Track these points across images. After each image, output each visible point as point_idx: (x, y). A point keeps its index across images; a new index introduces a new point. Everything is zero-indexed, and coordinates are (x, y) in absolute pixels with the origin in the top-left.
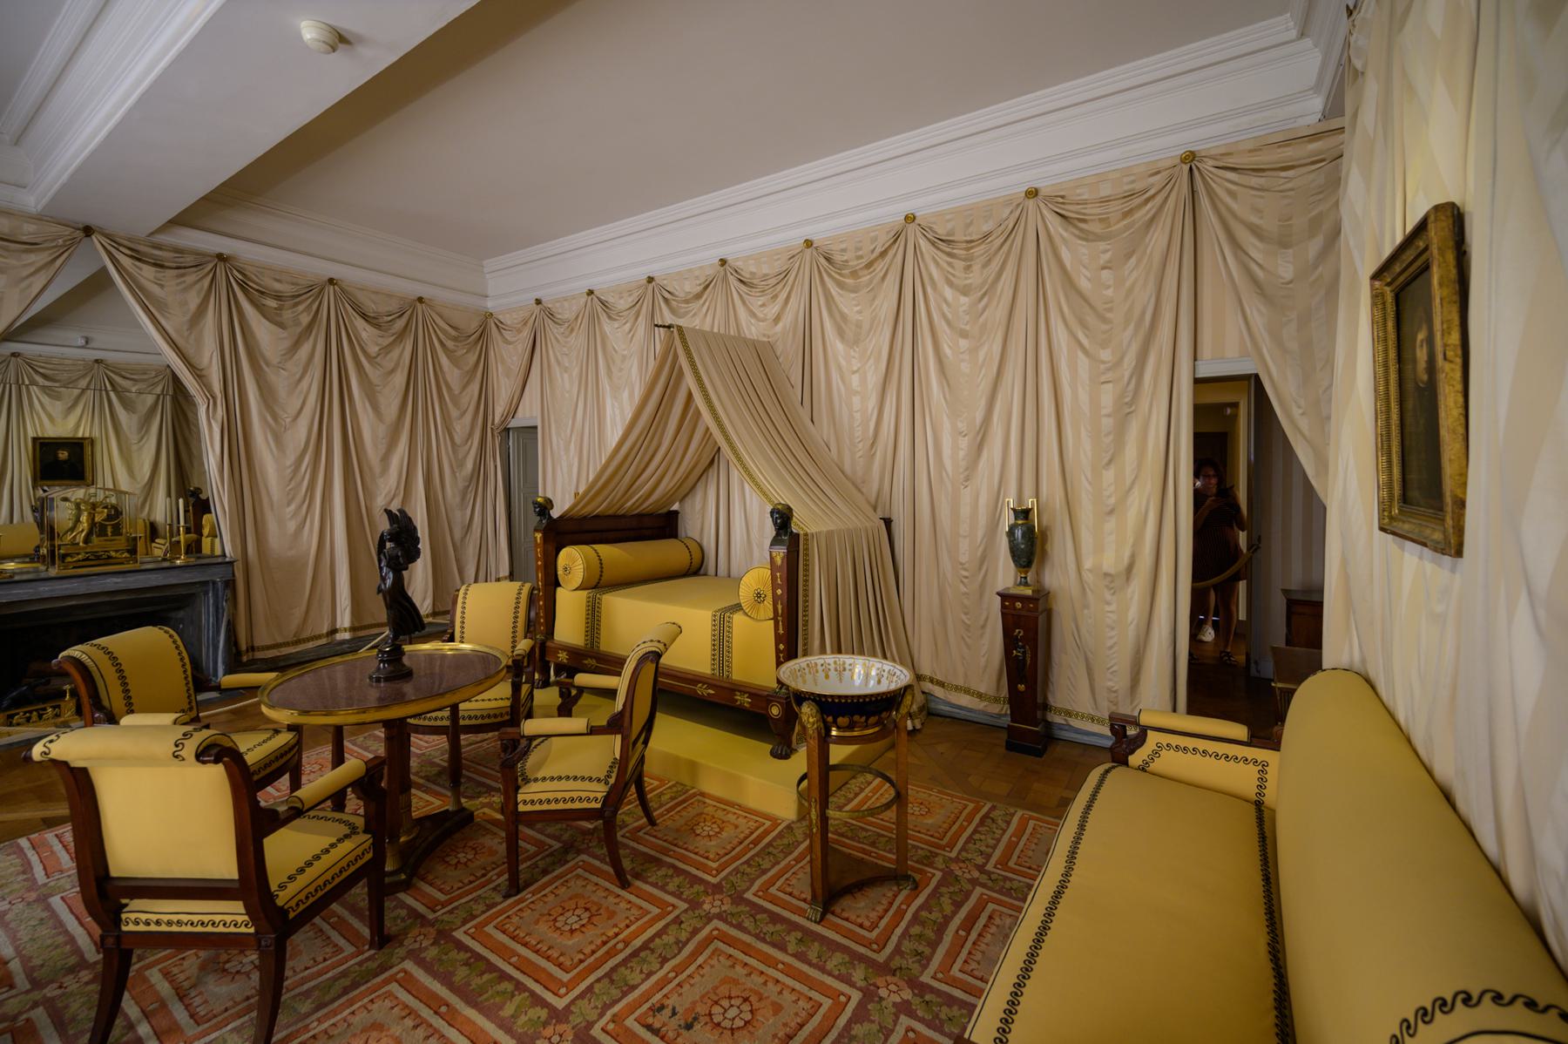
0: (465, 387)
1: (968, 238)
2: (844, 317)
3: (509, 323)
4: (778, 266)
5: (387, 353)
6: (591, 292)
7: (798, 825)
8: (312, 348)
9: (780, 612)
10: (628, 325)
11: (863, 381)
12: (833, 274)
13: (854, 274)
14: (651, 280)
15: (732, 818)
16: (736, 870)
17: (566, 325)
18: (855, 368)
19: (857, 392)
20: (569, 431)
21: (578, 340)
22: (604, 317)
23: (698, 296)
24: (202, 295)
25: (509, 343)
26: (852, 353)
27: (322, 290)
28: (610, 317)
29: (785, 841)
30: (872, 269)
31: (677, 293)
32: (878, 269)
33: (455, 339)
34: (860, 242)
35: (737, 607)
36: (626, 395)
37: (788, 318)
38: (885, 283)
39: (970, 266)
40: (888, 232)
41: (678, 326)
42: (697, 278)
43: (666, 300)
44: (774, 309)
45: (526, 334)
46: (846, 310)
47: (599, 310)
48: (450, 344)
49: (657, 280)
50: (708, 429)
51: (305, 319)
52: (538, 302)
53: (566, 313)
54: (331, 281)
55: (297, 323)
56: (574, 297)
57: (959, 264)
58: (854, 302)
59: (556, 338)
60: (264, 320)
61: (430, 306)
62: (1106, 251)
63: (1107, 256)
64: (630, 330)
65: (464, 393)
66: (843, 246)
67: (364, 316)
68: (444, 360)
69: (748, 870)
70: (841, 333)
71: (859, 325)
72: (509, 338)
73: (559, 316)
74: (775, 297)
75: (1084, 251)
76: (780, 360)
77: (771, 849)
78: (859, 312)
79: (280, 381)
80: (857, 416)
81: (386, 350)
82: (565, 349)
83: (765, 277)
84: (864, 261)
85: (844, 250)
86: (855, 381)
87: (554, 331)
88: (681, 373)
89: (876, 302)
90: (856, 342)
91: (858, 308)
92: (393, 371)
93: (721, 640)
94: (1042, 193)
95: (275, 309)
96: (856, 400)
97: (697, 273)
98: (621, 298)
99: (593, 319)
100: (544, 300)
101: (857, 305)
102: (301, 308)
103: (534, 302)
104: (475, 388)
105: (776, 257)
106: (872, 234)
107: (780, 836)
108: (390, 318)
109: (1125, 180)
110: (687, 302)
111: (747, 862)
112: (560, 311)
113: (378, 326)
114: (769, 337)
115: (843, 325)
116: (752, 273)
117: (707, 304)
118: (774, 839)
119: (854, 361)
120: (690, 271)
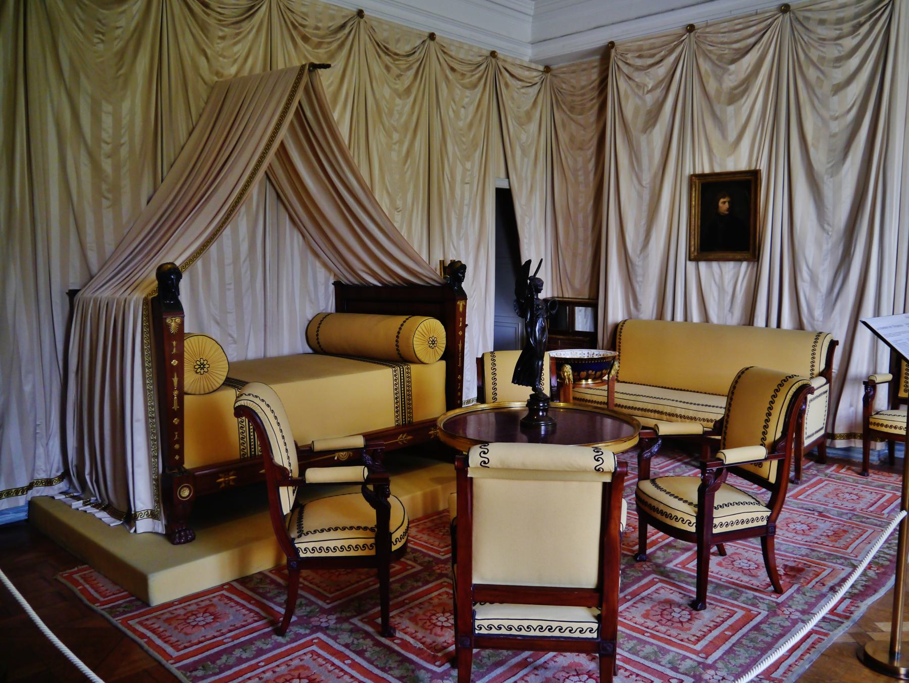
1: (398, 52)
34: (320, 13)
39: (401, 75)
57: (395, 71)
62: (467, 97)
63: (466, 100)
66: (304, 10)
75: (458, 92)
94: (437, 38)
109: (471, 53)
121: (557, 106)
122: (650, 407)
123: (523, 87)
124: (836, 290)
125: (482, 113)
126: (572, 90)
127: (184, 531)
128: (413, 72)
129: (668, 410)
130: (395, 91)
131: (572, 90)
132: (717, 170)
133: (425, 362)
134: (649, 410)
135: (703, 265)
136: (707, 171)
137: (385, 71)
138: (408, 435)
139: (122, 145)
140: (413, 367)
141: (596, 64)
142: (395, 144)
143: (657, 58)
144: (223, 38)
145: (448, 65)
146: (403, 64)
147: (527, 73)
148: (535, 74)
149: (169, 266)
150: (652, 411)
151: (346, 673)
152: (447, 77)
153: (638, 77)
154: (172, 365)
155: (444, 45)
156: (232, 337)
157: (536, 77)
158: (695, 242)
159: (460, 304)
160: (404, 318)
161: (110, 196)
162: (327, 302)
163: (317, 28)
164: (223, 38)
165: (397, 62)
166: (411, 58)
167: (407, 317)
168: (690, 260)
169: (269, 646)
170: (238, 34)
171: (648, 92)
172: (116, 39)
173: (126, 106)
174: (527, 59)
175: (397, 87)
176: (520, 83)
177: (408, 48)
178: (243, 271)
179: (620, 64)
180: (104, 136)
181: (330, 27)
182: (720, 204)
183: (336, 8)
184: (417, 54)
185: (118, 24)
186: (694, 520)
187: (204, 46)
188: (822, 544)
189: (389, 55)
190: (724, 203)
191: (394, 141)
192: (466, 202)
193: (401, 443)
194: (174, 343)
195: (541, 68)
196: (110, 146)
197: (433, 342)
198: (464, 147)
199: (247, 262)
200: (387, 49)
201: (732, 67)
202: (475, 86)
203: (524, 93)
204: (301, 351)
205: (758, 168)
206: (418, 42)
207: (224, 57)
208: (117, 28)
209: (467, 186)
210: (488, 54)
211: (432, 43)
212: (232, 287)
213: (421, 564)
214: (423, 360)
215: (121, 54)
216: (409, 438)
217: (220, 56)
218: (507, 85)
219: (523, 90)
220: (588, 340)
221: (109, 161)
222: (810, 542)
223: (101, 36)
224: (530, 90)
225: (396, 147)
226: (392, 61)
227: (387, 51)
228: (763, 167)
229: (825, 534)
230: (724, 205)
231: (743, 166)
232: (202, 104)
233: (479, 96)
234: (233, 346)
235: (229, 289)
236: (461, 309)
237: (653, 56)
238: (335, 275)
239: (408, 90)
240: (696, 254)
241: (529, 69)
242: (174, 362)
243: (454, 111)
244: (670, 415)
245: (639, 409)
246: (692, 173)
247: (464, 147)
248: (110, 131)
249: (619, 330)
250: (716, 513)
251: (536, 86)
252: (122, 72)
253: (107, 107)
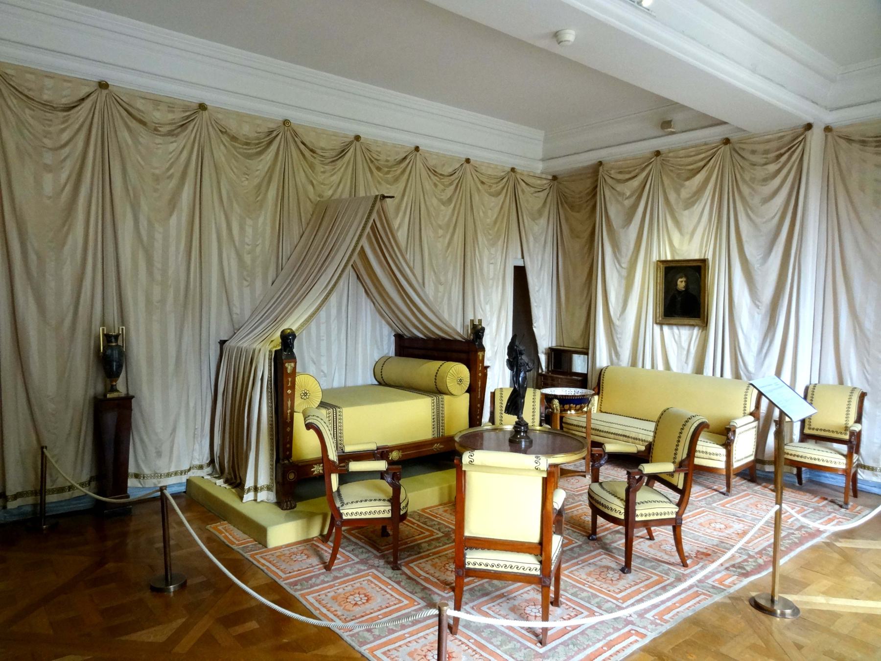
1: (443, 173)
34: (389, 151)
42: (258, 125)
57: (441, 187)
62: (493, 202)
63: (492, 204)
66: (379, 149)
94: (472, 162)
97: (259, 122)
121: (562, 207)
122: (620, 432)
123: (536, 192)
124: (764, 351)
125: (504, 213)
126: (573, 194)
127: (290, 501)
128: (453, 187)
129: (633, 435)
130: (441, 201)
131: (573, 194)
132: (677, 258)
133: (454, 394)
134: (619, 435)
135: (666, 328)
136: (669, 258)
137: (433, 187)
138: (441, 444)
139: (258, 245)
140: (446, 397)
141: (589, 175)
142: (440, 237)
143: (632, 174)
144: (324, 172)
145: (479, 180)
146: (446, 181)
147: (539, 182)
148: (545, 182)
149: (289, 331)
150: (621, 435)
151: (388, 593)
152: (478, 189)
153: (619, 187)
154: (288, 393)
155: (477, 166)
156: (323, 372)
157: (545, 184)
158: (660, 310)
159: (480, 354)
160: (440, 363)
161: (249, 279)
162: (389, 347)
163: (387, 161)
164: (324, 172)
165: (442, 180)
166: (451, 177)
167: (443, 362)
168: (657, 323)
169: (342, 575)
170: (334, 169)
171: (627, 198)
172: (256, 177)
173: (261, 220)
174: (539, 172)
175: (442, 197)
176: (533, 189)
177: (450, 170)
178: (333, 327)
179: (606, 177)
180: (247, 240)
181: (395, 160)
182: (679, 283)
183: (400, 146)
184: (456, 174)
185: (258, 168)
186: (623, 511)
187: (311, 178)
188: (731, 539)
189: (436, 176)
190: (682, 282)
191: (440, 235)
192: (491, 277)
194: (290, 379)
195: (550, 177)
196: (250, 247)
197: (461, 381)
198: (490, 237)
199: (336, 321)
200: (435, 172)
201: (687, 183)
202: (498, 194)
203: (536, 197)
204: (370, 383)
205: (706, 258)
206: (458, 166)
207: (325, 185)
208: (258, 170)
209: (492, 267)
210: (509, 170)
211: (467, 165)
212: (325, 338)
213: (442, 532)
214: (453, 393)
215: (259, 186)
216: (442, 446)
217: (322, 184)
218: (523, 191)
219: (536, 195)
220: (582, 381)
221: (249, 255)
222: (723, 536)
223: (247, 176)
224: (541, 194)
225: (441, 239)
226: (439, 180)
227: (435, 173)
228: (710, 257)
229: (736, 532)
230: (681, 284)
231: (697, 257)
232: (309, 216)
233: (502, 200)
234: (324, 378)
235: (323, 340)
236: (481, 358)
237: (630, 172)
238: (395, 331)
239: (450, 200)
240: (660, 319)
241: (540, 178)
242: (289, 391)
243: (483, 212)
244: (634, 439)
245: (612, 433)
246: (658, 259)
247: (490, 237)
248: (250, 237)
249: (602, 373)
250: (637, 507)
251: (545, 191)
252: (259, 199)
253: (249, 222)
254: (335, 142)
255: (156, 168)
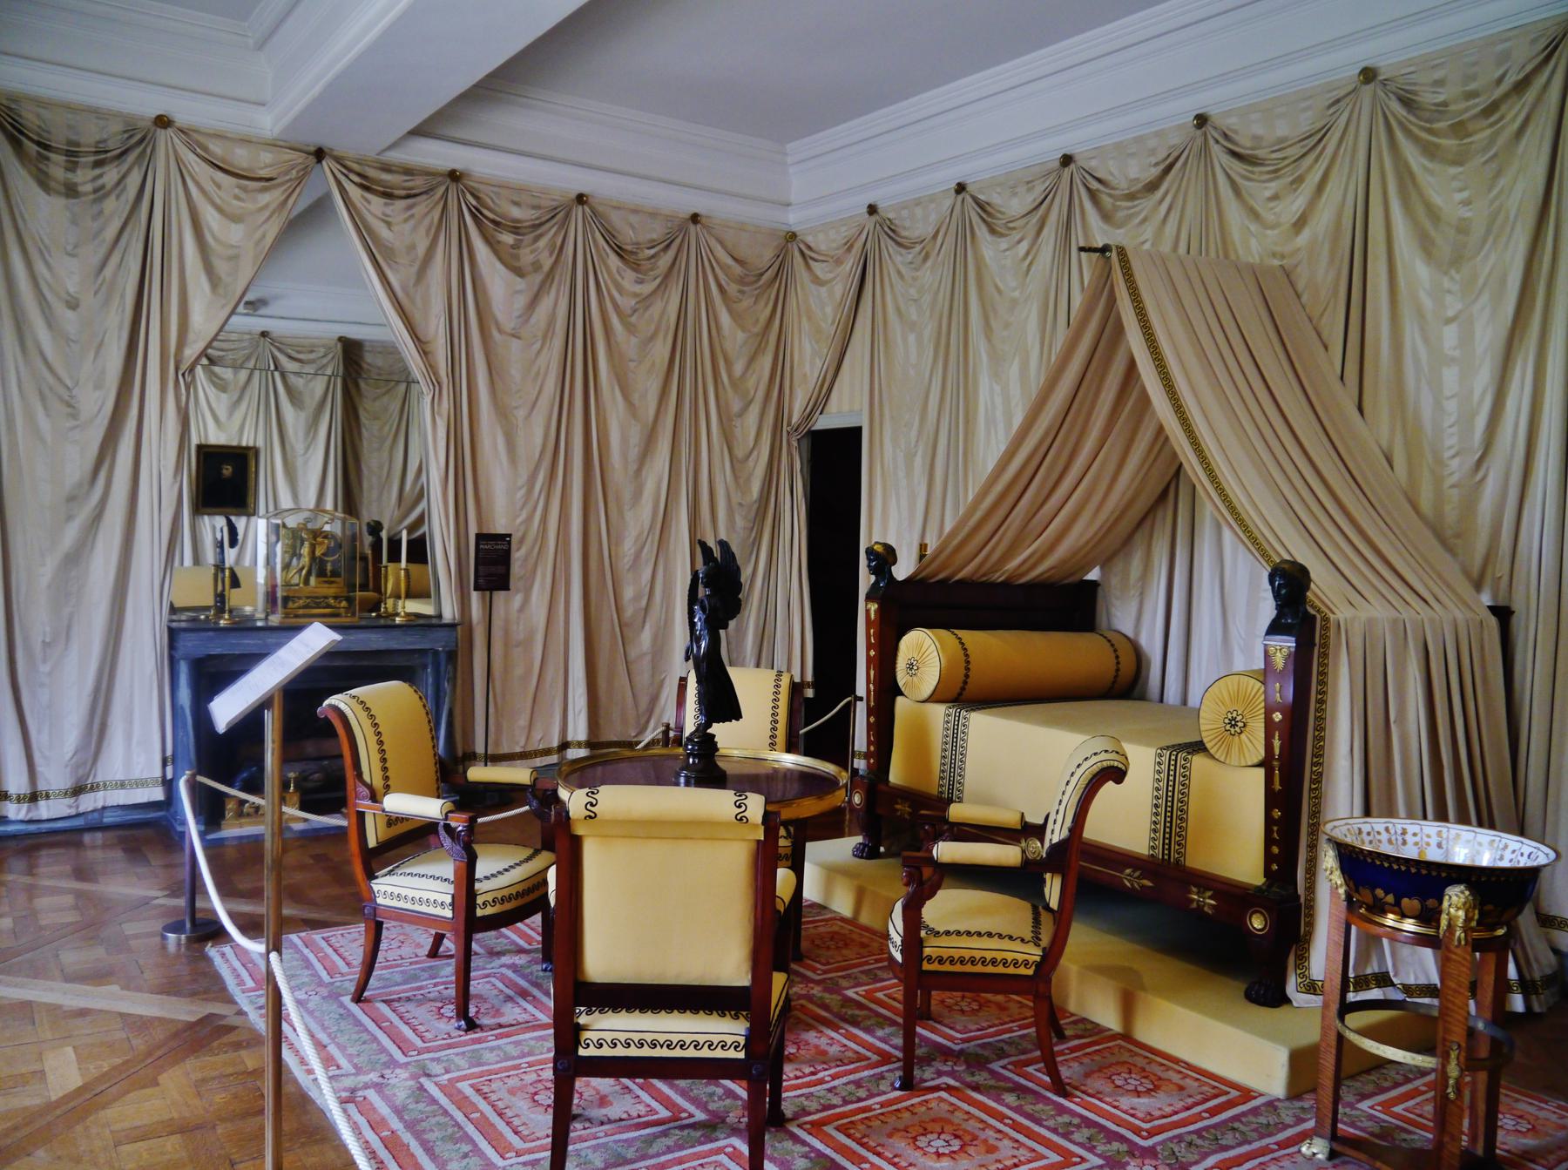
0: (752, 360)
2: (1434, 214)
3: (823, 248)
4: (1306, 122)
5: (647, 308)
6: (961, 188)
7: (1287, 1104)
8: (554, 303)
9: (1277, 751)
10: (1024, 246)
11: (1466, 339)
12: (1416, 130)
13: (1459, 129)
14: (1067, 160)
15: (1172, 1075)
16: (1180, 1138)
17: (918, 248)
18: (1450, 313)
19: (1453, 360)
20: (914, 433)
21: (932, 276)
22: (982, 231)
23: (1152, 186)
24: (431, 238)
25: (818, 281)
26: (1446, 283)
27: (567, 215)
28: (992, 231)
29: (1263, 1120)
30: (1492, 119)
31: (1114, 182)
32: (1508, 118)
33: (741, 281)
34: (1475, 64)
35: (1198, 747)
36: (1014, 371)
37: (1323, 218)
38: (1524, 141)
40: (1534, 41)
41: (1117, 247)
42: (1153, 152)
43: (1093, 195)
44: (1296, 204)
45: (850, 265)
46: (1437, 200)
47: (976, 219)
48: (732, 289)
49: (1081, 161)
50: (1161, 429)
51: (547, 263)
52: (872, 210)
53: (918, 227)
54: (581, 199)
55: (537, 266)
56: (932, 199)
58: (1455, 184)
59: (899, 272)
60: (499, 265)
61: (704, 226)
64: (1028, 254)
65: (750, 371)
67: (620, 251)
68: (725, 319)
69: (1199, 1142)
70: (1426, 245)
71: (1463, 228)
72: (819, 273)
73: (905, 233)
74: (1299, 180)
76: (1305, 298)
77: (1236, 1125)
78: (1466, 203)
79: (514, 354)
80: (1451, 406)
81: (645, 301)
82: (913, 291)
83: (1281, 144)
84: (1482, 102)
85: (1439, 83)
86: (1450, 335)
87: (896, 260)
88: (1119, 330)
89: (1502, 182)
90: (1457, 261)
91: (1465, 194)
92: (653, 337)
93: (1170, 800)
95: (512, 247)
96: (1450, 376)
97: (1152, 143)
98: (1015, 194)
99: (965, 235)
100: (881, 206)
101: (1461, 190)
102: (542, 243)
103: (865, 210)
104: (766, 361)
105: (1303, 105)
106: (1500, 47)
107: (1255, 1111)
108: (652, 252)
110: (1131, 197)
111: (1198, 1132)
112: (907, 224)
113: (635, 267)
114: (1283, 257)
115: (1433, 233)
116: (1256, 138)
117: (1168, 199)
118: (1244, 1114)
119: (1449, 299)
120: (1139, 140)
185: (1142, 239)
193: (1128, 884)
254: (1309, 113)
255: (1014, 289)
